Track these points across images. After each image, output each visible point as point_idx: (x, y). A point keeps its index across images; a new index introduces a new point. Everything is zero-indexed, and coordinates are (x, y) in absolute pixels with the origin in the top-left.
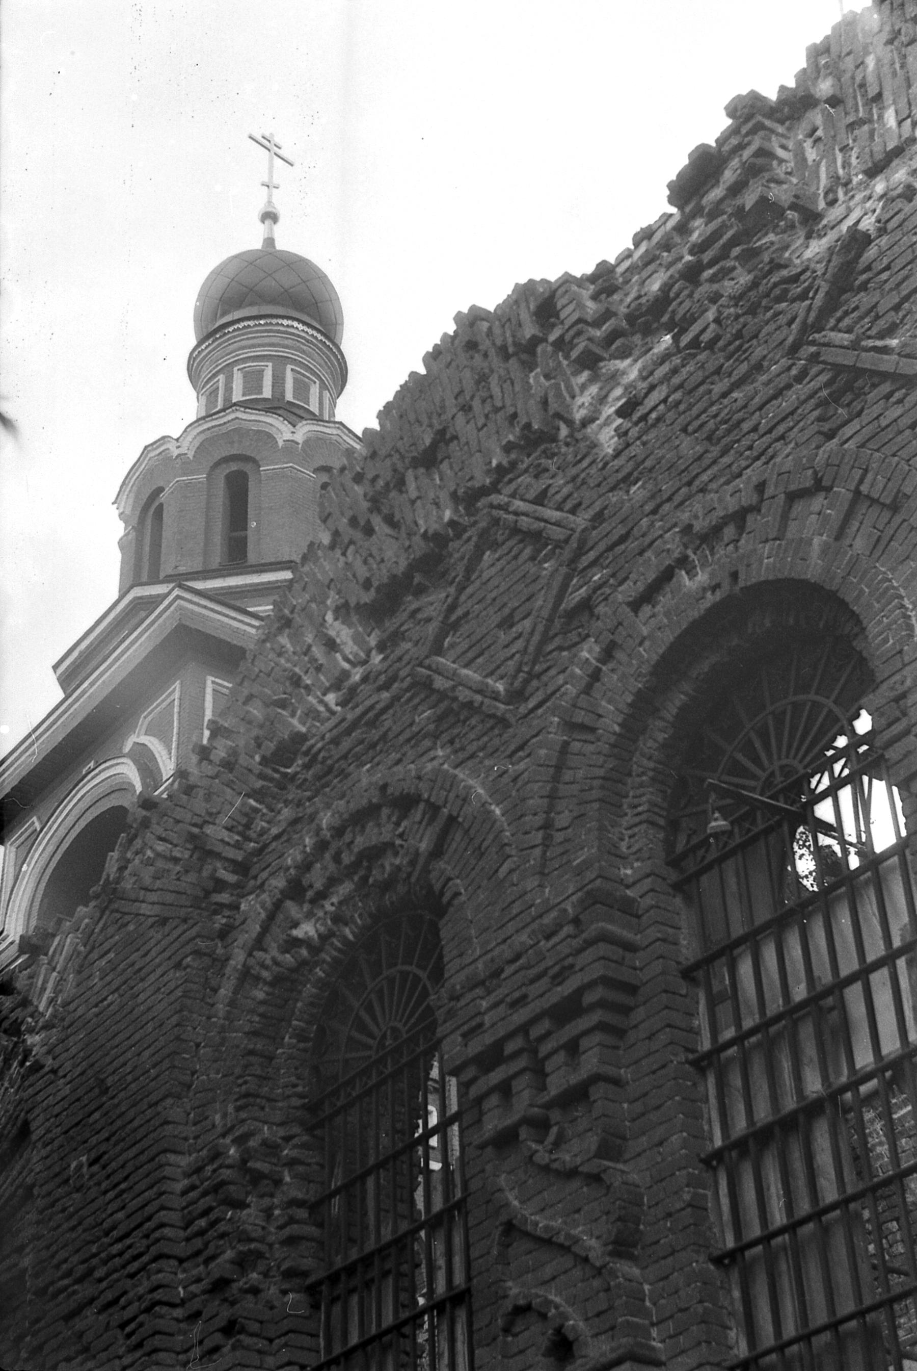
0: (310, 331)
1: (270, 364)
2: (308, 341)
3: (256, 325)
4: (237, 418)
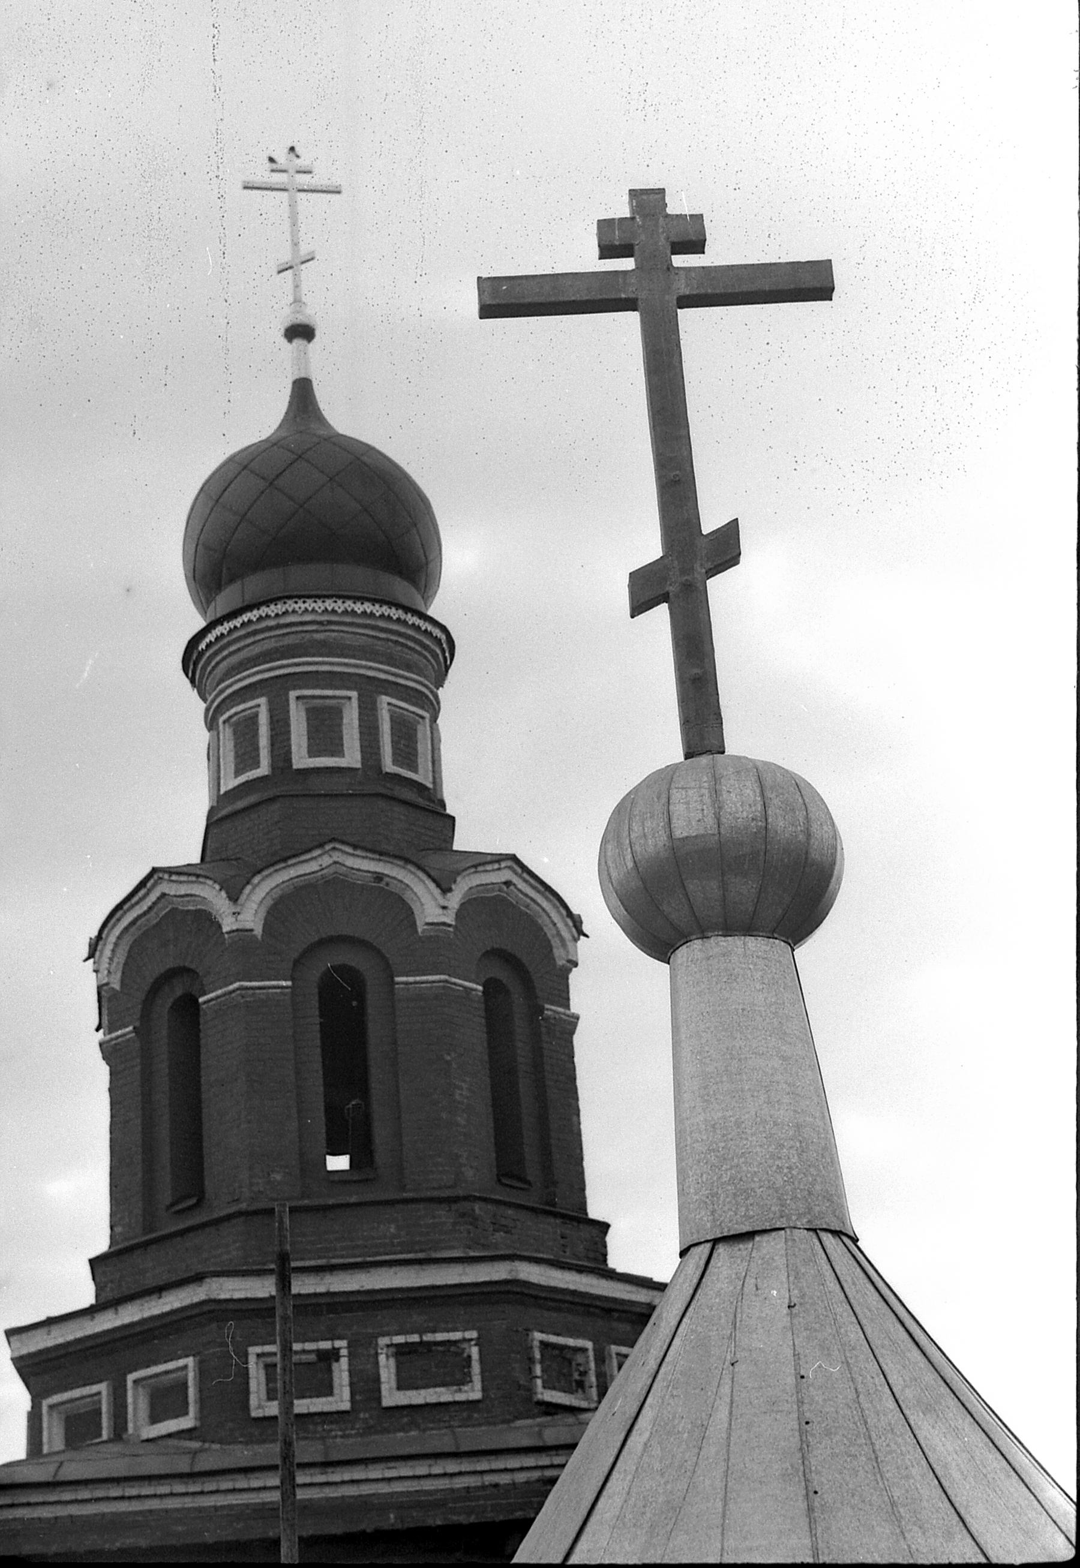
1: (262, 701)
2: (321, 623)
4: (164, 895)
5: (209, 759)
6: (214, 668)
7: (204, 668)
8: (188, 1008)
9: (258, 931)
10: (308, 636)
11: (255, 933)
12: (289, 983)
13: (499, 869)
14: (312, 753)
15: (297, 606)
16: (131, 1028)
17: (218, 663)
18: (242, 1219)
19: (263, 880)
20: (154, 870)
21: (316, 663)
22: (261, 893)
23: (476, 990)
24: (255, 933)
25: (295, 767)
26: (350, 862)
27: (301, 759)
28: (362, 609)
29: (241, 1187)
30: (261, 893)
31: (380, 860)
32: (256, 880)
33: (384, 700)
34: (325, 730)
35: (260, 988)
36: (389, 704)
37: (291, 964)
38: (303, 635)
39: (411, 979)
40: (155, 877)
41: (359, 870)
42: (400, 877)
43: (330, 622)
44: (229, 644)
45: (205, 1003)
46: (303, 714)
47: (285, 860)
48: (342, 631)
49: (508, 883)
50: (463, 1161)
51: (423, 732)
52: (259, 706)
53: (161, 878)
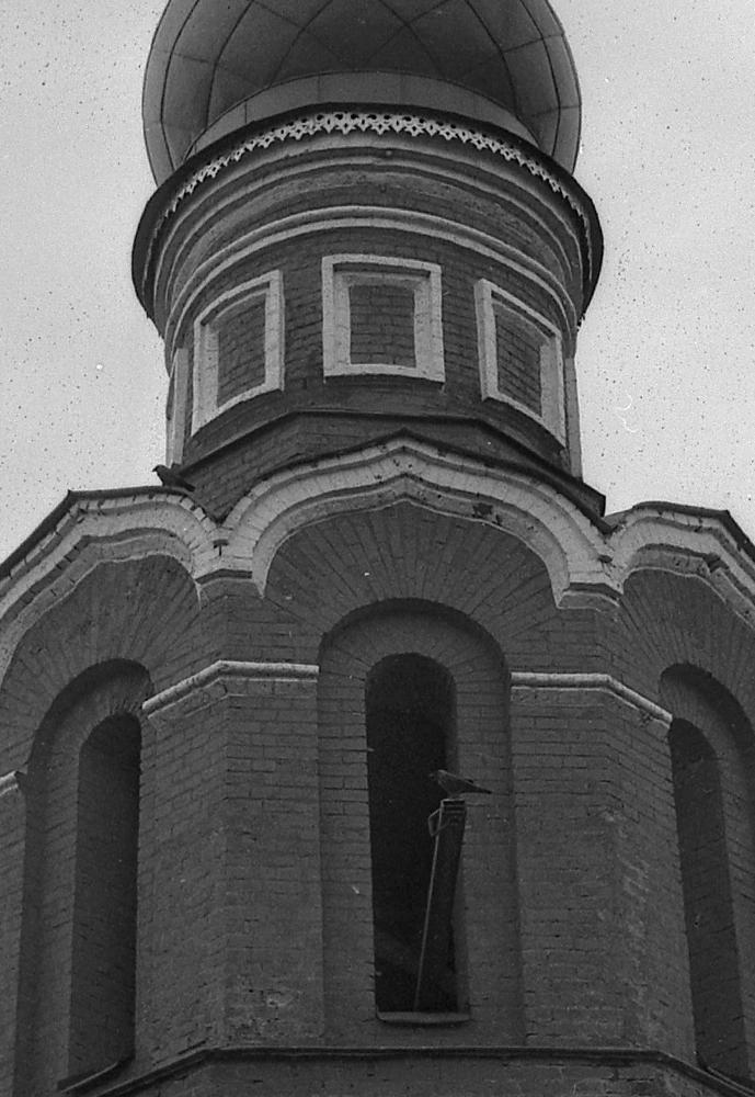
0: (380, 123)
1: (274, 276)
2: (381, 154)
3: (223, 172)
4: (87, 540)
5: (169, 418)
6: (189, 247)
7: (171, 253)
8: (121, 747)
9: (260, 578)
10: (356, 176)
11: (254, 580)
12: (316, 668)
13: (698, 530)
14: (357, 356)
15: (341, 124)
16: (12, 774)
17: (197, 236)
18: (204, 1073)
19: (273, 491)
20: (73, 497)
21: (371, 215)
22: (266, 515)
23: (659, 716)
24: (254, 580)
25: (326, 374)
26: (433, 475)
27: (337, 359)
28: (453, 135)
29: (207, 1020)
30: (266, 515)
31: (487, 475)
32: (259, 490)
33: (487, 286)
34: (381, 318)
35: (258, 673)
36: (494, 295)
37: (317, 642)
38: (350, 173)
39: (542, 677)
40: (74, 510)
41: (448, 490)
42: (522, 506)
43: (396, 154)
44: (220, 196)
45: (152, 709)
46: (344, 299)
47: (313, 461)
48: (417, 172)
49: (713, 561)
50: (639, 1000)
51: (550, 354)
52: (267, 285)
53: (82, 511)
